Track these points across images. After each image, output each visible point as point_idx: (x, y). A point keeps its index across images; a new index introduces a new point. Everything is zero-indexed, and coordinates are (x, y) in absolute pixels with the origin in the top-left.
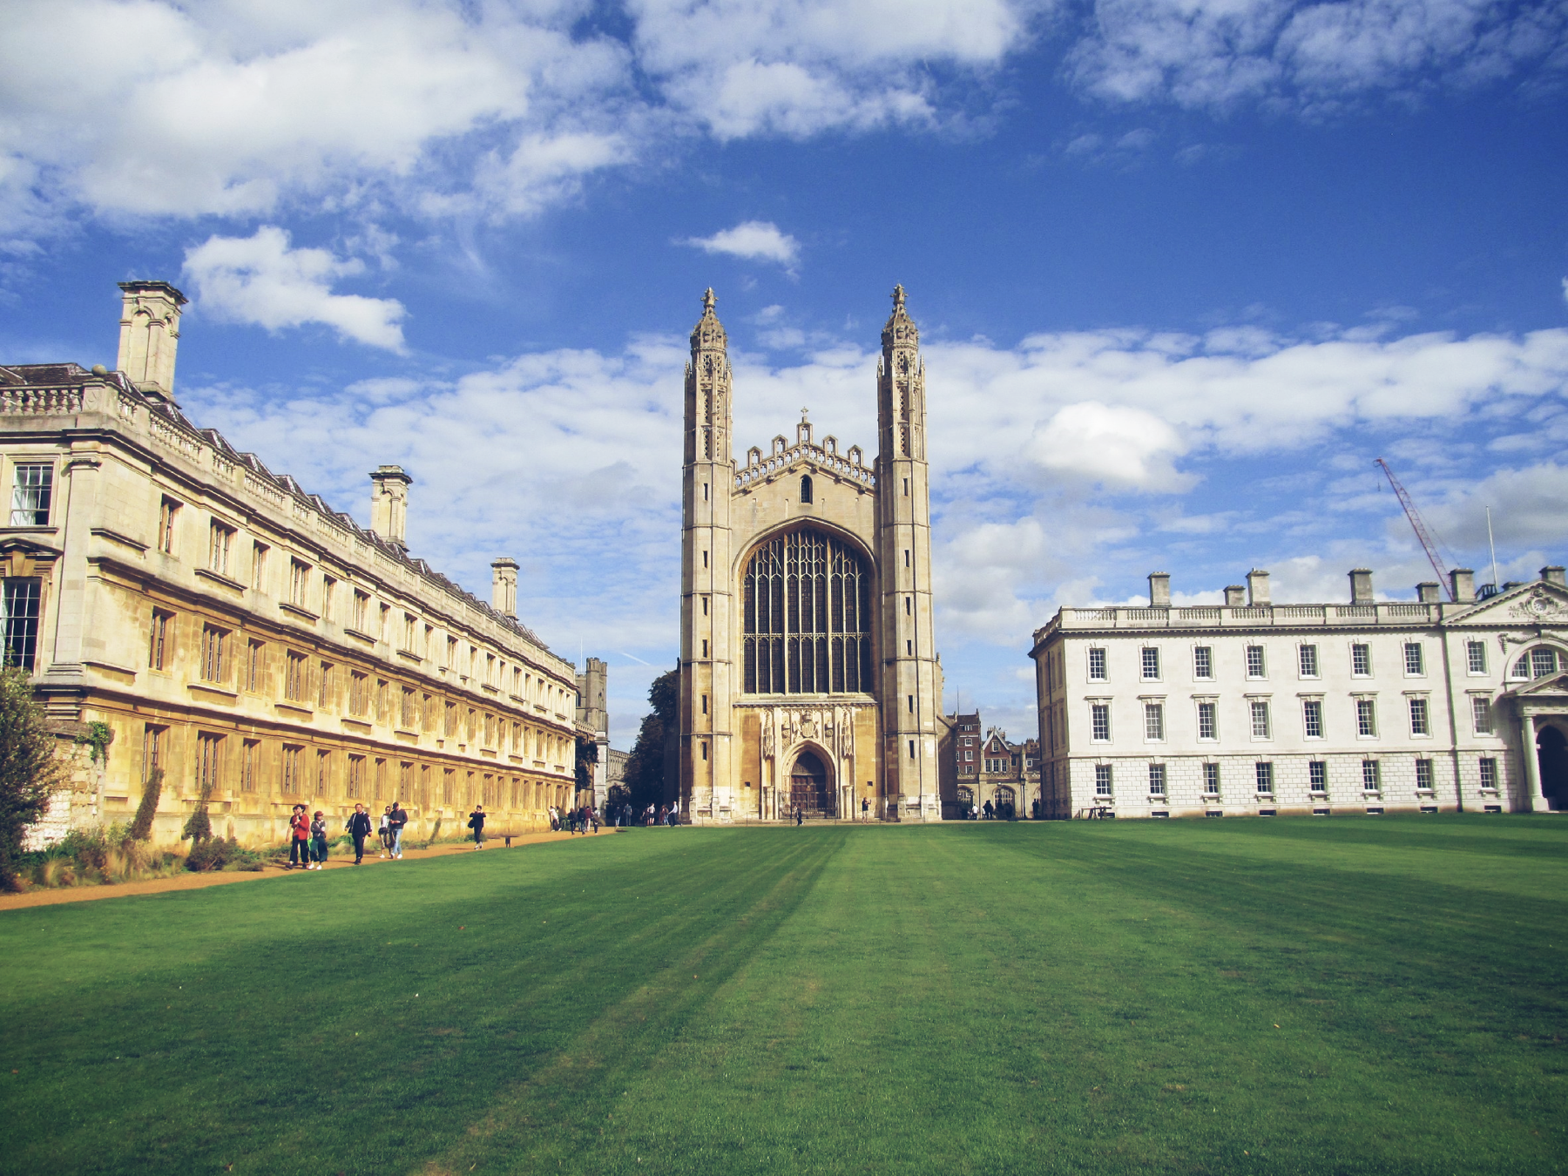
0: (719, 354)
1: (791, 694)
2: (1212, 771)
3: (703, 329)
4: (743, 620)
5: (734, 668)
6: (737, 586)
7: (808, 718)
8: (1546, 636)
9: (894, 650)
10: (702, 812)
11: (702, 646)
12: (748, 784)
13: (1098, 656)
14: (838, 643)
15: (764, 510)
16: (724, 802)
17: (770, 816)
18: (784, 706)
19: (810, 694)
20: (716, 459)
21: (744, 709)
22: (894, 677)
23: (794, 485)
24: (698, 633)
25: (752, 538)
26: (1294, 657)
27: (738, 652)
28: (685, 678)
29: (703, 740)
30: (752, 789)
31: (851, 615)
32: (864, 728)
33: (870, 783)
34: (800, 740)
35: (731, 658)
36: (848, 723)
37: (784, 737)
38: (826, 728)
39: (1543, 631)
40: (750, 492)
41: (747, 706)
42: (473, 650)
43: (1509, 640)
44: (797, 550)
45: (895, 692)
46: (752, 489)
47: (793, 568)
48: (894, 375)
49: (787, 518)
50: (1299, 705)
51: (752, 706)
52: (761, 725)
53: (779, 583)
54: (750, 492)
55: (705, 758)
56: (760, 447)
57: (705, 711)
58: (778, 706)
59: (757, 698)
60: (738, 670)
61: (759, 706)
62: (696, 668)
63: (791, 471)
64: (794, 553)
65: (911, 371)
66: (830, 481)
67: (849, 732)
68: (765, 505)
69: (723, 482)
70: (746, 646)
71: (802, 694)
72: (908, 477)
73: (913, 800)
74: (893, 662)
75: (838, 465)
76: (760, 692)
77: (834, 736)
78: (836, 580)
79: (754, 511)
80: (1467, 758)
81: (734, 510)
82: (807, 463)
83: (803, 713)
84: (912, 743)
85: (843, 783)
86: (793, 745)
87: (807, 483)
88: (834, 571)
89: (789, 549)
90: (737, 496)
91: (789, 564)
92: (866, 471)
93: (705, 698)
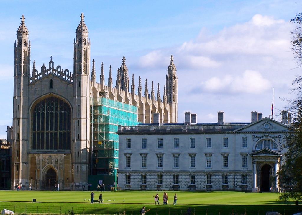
1: (46, 150)
2: (160, 177)
4: (32, 126)
8: (268, 136)
12: (32, 178)
14: (60, 133)
15: (38, 90)
17: (38, 188)
21: (31, 155)
25: (35, 100)
26: (189, 142)
27: (31, 136)
30: (33, 180)
34: (48, 165)
38: (55, 161)
39: (265, 135)
43: (255, 137)
47: (48, 109)
50: (188, 157)
51: (33, 154)
53: (43, 114)
55: (18, 170)
64: (48, 105)
68: (39, 89)
70: (33, 134)
73: (77, 184)
74: (74, 141)
76: (37, 149)
78: (61, 113)
79: (35, 91)
80: (238, 175)
84: (78, 167)
85: (59, 179)
86: (45, 167)
87: (52, 81)
90: (30, 86)
91: (47, 108)
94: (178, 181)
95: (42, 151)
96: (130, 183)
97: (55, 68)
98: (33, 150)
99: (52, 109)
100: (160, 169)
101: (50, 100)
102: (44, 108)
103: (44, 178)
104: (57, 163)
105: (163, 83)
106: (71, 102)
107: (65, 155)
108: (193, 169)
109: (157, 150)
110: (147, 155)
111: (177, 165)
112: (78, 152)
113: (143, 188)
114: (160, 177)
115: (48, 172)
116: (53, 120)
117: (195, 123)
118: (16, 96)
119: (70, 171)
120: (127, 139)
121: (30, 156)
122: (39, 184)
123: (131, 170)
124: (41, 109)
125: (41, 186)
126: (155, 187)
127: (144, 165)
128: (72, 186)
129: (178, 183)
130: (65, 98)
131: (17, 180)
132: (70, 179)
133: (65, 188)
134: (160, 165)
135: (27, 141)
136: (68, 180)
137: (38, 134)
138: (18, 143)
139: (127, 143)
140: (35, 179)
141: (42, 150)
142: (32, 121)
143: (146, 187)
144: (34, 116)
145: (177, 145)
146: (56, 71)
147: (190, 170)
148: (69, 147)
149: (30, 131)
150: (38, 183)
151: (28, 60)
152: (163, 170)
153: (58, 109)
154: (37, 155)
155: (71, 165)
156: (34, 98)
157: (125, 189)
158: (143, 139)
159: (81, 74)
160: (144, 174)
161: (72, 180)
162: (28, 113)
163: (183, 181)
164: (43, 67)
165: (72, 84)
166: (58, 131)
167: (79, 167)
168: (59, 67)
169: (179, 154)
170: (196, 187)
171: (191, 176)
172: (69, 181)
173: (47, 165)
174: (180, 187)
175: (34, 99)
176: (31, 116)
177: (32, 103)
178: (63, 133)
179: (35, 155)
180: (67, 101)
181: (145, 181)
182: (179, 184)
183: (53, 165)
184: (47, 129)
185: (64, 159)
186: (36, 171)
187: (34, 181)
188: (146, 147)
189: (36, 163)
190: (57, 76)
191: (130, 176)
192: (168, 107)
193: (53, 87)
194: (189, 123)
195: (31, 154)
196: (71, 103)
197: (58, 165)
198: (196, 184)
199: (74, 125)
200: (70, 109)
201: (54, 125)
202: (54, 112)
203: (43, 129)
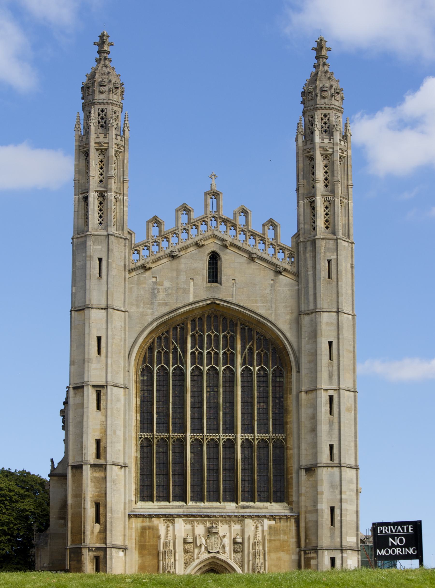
0: (115, 108)
3: (98, 78)
5: (130, 472)
6: (133, 377)
7: (214, 530)
9: (315, 455)
11: (94, 446)
18: (187, 516)
20: (112, 230)
21: (140, 519)
22: (315, 486)
24: (90, 431)
25: (151, 323)
28: (74, 482)
29: (95, 554)
31: (263, 412)
32: (277, 543)
34: (206, 556)
35: (127, 461)
36: (259, 537)
37: (186, 551)
38: (235, 543)
40: (150, 268)
41: (143, 516)
44: (202, 337)
45: (315, 502)
46: (153, 266)
48: (317, 139)
49: (191, 300)
51: (150, 516)
52: (159, 537)
54: (150, 268)
56: (161, 217)
57: (98, 520)
58: (180, 516)
60: (133, 474)
61: (158, 516)
62: (87, 472)
63: (198, 245)
65: (337, 137)
67: (261, 548)
68: (167, 284)
70: (142, 447)
71: (207, 504)
72: (333, 257)
75: (251, 242)
76: (158, 500)
77: (243, 551)
79: (153, 293)
81: (131, 289)
82: (215, 237)
83: (208, 525)
84: (333, 560)
86: (197, 562)
88: (244, 363)
89: (193, 336)
90: (134, 273)
91: (193, 353)
92: (283, 249)
93: (97, 505)
95: (180, 507)
98: (141, 504)
102: (184, 351)
106: (288, 335)
107: (273, 522)
124: (171, 355)
138: (98, 474)
149: (134, 435)
153: (239, 360)
154: (162, 519)
167: (338, 563)
175: (150, 319)
176: (136, 382)
179: (155, 521)
185: (270, 534)
199: (305, 413)
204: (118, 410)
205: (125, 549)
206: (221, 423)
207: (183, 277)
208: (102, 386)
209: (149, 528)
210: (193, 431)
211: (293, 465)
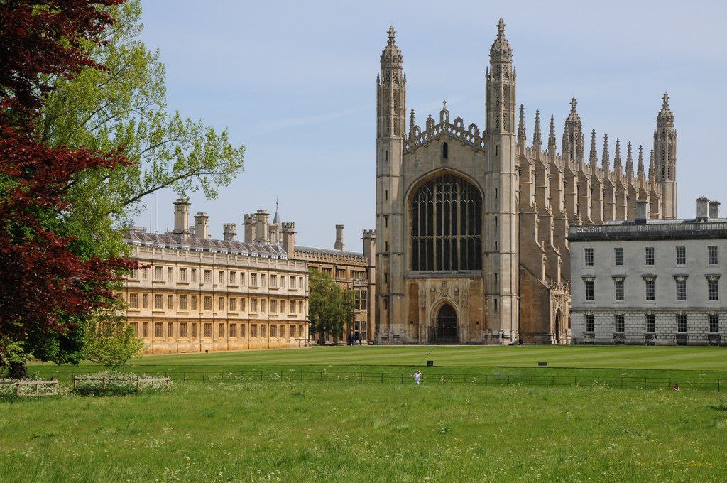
2: (651, 320)
4: (411, 228)
10: (384, 338)
12: (412, 323)
13: (589, 252)
14: (463, 241)
15: (422, 164)
16: (396, 333)
17: (423, 341)
19: (447, 271)
20: (393, 135)
21: (409, 280)
23: (436, 149)
26: (705, 254)
27: (409, 246)
30: (414, 325)
31: (471, 224)
33: (477, 323)
37: (432, 296)
42: (221, 273)
47: (439, 197)
48: (492, 79)
49: (434, 167)
50: (706, 282)
51: (415, 279)
53: (431, 206)
57: (386, 282)
59: (417, 273)
64: (439, 189)
66: (459, 145)
68: (422, 161)
69: (396, 149)
73: (495, 333)
74: (487, 254)
76: (421, 270)
78: (463, 204)
79: (416, 165)
84: (496, 300)
87: (445, 146)
89: (437, 186)
93: (386, 274)
94: (685, 326)
96: (593, 331)
97: (452, 122)
98: (412, 272)
99: (447, 197)
100: (650, 304)
101: (443, 181)
103: (433, 321)
104: (458, 295)
105: (649, 145)
108: (715, 304)
109: (644, 270)
110: (624, 278)
111: (682, 296)
112: (496, 275)
113: (618, 339)
114: (651, 320)
115: (441, 312)
116: (449, 217)
117: (717, 217)
118: (382, 175)
119: (481, 309)
120: (586, 250)
121: (408, 282)
122: (425, 333)
123: (595, 306)
125: (429, 337)
126: (642, 337)
127: (620, 296)
128: (486, 337)
129: (685, 331)
130: (470, 176)
131: (386, 325)
132: (482, 324)
133: (473, 340)
134: (651, 297)
135: (402, 256)
136: (477, 325)
137: (423, 241)
139: (586, 257)
140: (417, 324)
141: (430, 272)
142: (412, 220)
143: (623, 336)
144: (414, 210)
145: (681, 260)
146: (453, 127)
147: (709, 306)
148: (479, 266)
150: (423, 332)
151: (399, 110)
152: (656, 306)
153: (459, 197)
155: (482, 298)
156: (413, 177)
157: (584, 341)
158: (616, 249)
159: (500, 131)
160: (619, 314)
161: (486, 326)
162: (403, 205)
163: (695, 326)
164: (430, 121)
165: (484, 152)
166: (459, 237)
167: (498, 302)
168: (459, 120)
169: (686, 277)
170: (720, 338)
171: (711, 318)
172: (479, 329)
173: (439, 298)
174: (690, 338)
175: (414, 179)
177: (411, 184)
178: (467, 240)
179: (417, 281)
180: (474, 182)
181: (621, 326)
182: (688, 332)
183: (451, 299)
184: (439, 233)
186: (420, 309)
187: (415, 327)
188: (622, 264)
189: (419, 294)
190: (453, 138)
191: (593, 318)
192: (657, 191)
193: (449, 156)
194: (705, 219)
195: (409, 278)
196: (483, 186)
197: (460, 299)
198: (720, 332)
200: (480, 195)
201: (451, 226)
202: (450, 202)
203: (431, 233)
204: (397, 227)
205: (402, 295)
206: (451, 230)
207: (429, 158)
208: (388, 216)
209: (415, 284)
210: (437, 234)
211: (483, 251)
